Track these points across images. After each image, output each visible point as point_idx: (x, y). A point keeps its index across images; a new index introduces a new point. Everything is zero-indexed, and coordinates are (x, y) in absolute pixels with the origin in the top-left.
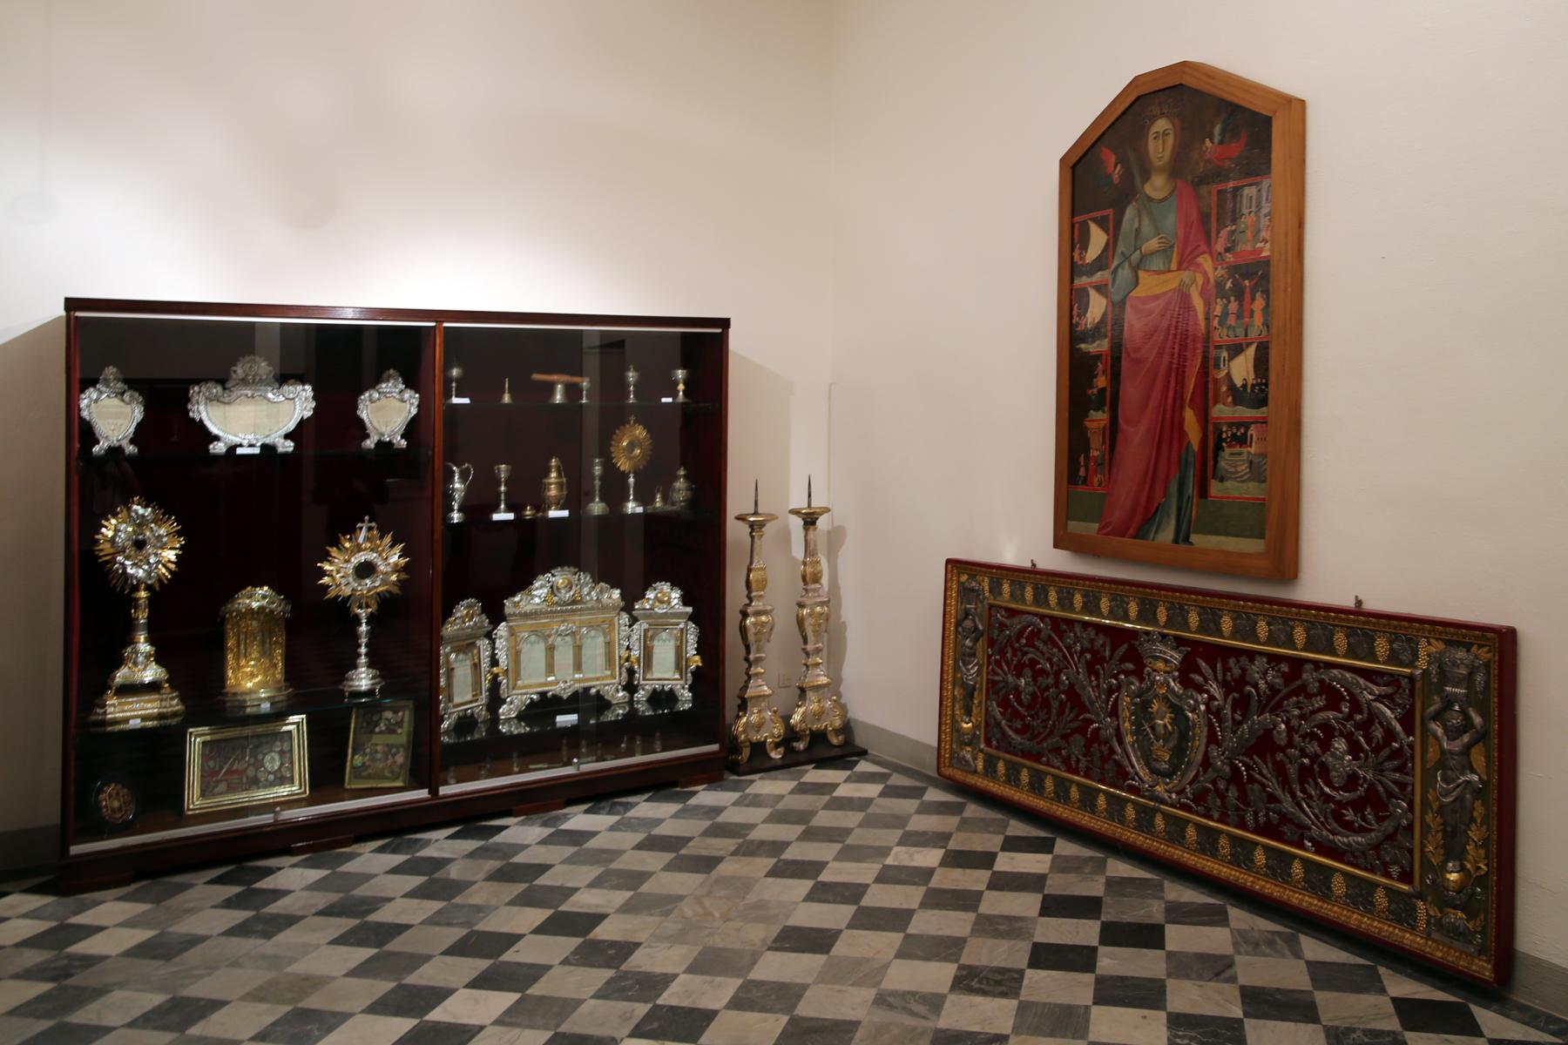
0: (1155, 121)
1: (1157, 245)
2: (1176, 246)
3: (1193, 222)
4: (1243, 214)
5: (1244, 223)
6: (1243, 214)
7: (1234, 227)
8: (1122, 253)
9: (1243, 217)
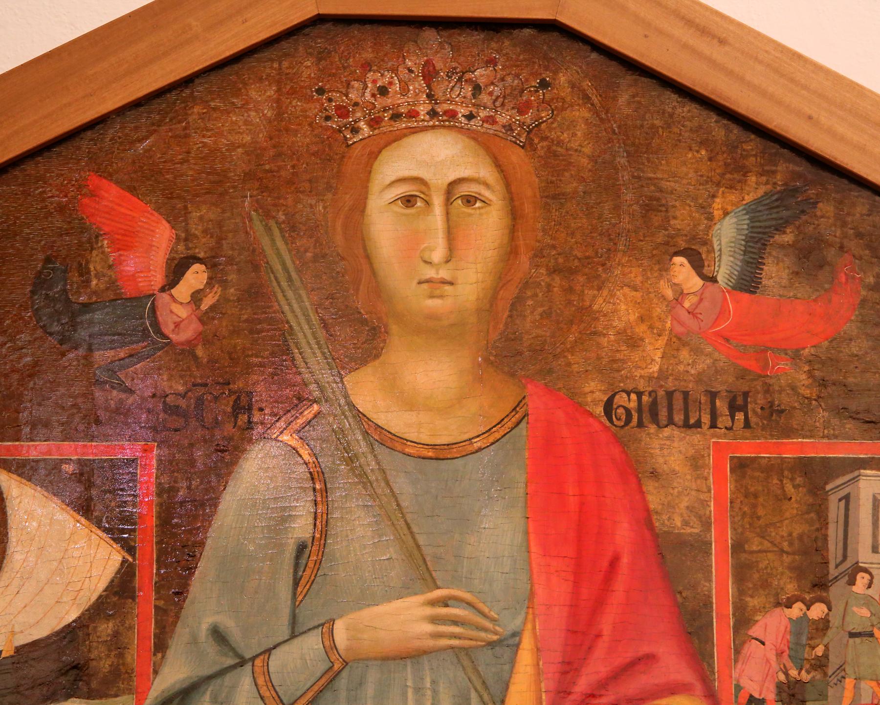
0: (399, 137)
1: (429, 628)
2: (527, 643)
3: (614, 562)
4: (857, 569)
5: (868, 601)
6: (857, 569)
7: (817, 611)
8: (218, 635)
9: (862, 579)
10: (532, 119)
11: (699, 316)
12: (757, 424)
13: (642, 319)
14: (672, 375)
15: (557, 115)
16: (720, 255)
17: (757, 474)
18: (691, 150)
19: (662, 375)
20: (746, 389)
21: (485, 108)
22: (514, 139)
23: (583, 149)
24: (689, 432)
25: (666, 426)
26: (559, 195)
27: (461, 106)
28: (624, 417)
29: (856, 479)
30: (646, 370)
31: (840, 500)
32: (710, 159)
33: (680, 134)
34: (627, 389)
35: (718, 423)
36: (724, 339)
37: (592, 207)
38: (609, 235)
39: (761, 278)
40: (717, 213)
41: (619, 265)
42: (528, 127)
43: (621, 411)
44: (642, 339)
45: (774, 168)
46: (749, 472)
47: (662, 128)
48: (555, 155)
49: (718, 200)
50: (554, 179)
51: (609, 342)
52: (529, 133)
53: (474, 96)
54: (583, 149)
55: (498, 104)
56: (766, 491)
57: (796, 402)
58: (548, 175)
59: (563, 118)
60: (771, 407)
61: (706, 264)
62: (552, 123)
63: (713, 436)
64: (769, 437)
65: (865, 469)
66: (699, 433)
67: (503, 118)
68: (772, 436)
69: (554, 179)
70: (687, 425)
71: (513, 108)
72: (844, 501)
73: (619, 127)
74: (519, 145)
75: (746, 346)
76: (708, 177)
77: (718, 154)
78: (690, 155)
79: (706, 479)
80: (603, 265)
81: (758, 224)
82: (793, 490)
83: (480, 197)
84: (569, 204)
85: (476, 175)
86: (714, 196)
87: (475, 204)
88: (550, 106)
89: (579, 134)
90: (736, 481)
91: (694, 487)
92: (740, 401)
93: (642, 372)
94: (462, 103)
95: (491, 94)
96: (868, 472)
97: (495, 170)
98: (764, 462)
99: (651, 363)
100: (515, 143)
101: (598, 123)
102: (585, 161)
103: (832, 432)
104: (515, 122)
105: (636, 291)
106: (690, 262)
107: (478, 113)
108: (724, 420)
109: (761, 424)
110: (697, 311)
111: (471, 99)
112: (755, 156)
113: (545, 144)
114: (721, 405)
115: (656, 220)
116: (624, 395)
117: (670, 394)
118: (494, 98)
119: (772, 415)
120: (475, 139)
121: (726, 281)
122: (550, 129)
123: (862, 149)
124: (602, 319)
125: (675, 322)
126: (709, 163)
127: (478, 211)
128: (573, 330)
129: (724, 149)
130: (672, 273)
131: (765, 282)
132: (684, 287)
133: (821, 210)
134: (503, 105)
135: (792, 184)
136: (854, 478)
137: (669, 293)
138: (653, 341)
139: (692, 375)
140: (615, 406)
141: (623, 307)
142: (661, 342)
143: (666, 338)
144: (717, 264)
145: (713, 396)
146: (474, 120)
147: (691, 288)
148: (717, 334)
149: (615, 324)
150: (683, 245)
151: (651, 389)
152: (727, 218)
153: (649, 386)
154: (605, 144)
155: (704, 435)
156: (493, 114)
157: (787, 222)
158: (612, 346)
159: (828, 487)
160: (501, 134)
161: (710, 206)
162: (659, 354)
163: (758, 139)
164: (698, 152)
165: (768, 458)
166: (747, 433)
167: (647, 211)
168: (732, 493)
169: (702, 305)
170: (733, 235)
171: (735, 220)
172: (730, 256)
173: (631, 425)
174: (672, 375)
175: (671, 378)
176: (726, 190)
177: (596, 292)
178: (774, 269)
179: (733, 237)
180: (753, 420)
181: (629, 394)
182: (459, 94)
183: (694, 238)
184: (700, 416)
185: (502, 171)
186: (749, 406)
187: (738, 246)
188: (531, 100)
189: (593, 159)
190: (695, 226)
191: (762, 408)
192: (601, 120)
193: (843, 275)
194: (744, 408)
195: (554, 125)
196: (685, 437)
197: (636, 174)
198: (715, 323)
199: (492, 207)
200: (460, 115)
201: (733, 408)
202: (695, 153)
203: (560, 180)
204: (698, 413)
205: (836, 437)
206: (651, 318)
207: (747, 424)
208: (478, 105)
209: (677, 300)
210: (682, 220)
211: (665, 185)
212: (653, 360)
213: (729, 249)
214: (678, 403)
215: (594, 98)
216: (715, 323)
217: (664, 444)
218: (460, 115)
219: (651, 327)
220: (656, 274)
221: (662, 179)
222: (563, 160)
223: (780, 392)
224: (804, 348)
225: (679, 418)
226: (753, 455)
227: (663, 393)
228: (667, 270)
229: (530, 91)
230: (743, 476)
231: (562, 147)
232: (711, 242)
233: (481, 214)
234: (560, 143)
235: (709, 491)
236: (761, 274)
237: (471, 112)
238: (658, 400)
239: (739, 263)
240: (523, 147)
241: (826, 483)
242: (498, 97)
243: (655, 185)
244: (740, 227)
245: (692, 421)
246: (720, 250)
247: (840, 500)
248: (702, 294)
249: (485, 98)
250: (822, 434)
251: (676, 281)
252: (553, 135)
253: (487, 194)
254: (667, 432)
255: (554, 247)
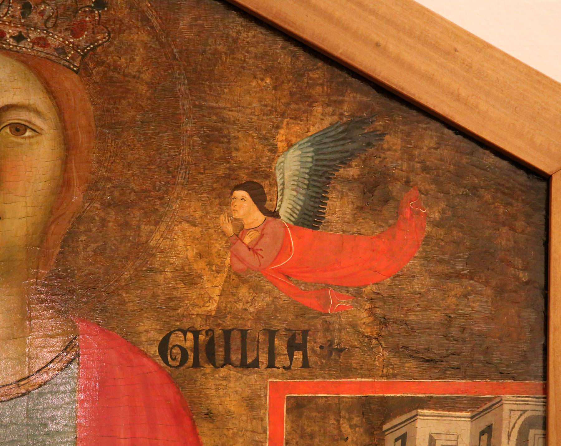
10: (86, 42)
11: (259, 252)
12: (316, 363)
13: (200, 255)
14: (230, 313)
15: (114, 38)
16: (283, 189)
17: (314, 414)
18: (255, 78)
19: (220, 313)
20: (306, 328)
21: (36, 29)
22: (67, 64)
23: (142, 76)
24: (246, 372)
25: (223, 366)
26: (115, 124)
27: (10, 25)
28: (179, 357)
29: (413, 419)
30: (204, 309)
31: (396, 440)
32: (275, 88)
33: (245, 61)
34: (183, 328)
35: (276, 362)
36: (285, 276)
37: (151, 138)
38: (168, 167)
39: (324, 213)
40: (281, 145)
41: (177, 199)
42: (83, 51)
43: (176, 350)
44: (200, 277)
45: (341, 98)
46: (306, 412)
47: (226, 54)
48: (112, 81)
49: (282, 131)
50: (110, 107)
51: (165, 279)
52: (83, 57)
53: (23, 15)
54: (142, 76)
55: (49, 24)
56: (322, 431)
57: (356, 340)
58: (104, 102)
59: (121, 42)
60: (330, 345)
61: (268, 198)
62: (109, 47)
63: (271, 376)
64: (327, 376)
65: (423, 408)
66: (256, 373)
67: (55, 40)
68: (331, 376)
69: (110, 107)
70: (244, 365)
71: (66, 29)
72: (400, 441)
73: (180, 52)
74: (73, 70)
75: (306, 283)
76: (272, 107)
77: (283, 82)
78: (254, 84)
79: (262, 420)
80: (161, 198)
81: (322, 157)
82: (349, 430)
83: (31, 126)
84: (125, 134)
85: (26, 102)
86: (278, 127)
87: (24, 133)
88: (107, 28)
89: (138, 59)
90: (292, 422)
91: (249, 427)
92: (299, 340)
93: (199, 311)
94: (10, 22)
95: (42, 13)
96: (426, 412)
97: (46, 96)
98: (321, 401)
99: (209, 301)
100: (69, 67)
101: (158, 47)
102: (143, 89)
103: (391, 371)
104: (68, 45)
105: (195, 225)
106: (251, 196)
107: (28, 34)
108: (282, 360)
109: (319, 363)
110: (258, 247)
111: (20, 19)
112: (322, 85)
113: (101, 69)
114: (280, 344)
115: (217, 151)
116: (181, 334)
117: (227, 334)
118: (45, 17)
119: (331, 354)
120: (23, 62)
121: (289, 216)
122: (107, 54)
123: (430, 79)
124: (159, 255)
125: (235, 259)
126: (274, 92)
127: (28, 141)
128: (128, 267)
129: (290, 77)
130: (233, 208)
131: (328, 217)
132: (245, 222)
133: (388, 143)
134: (55, 25)
135: (359, 114)
136: (411, 418)
137: (229, 229)
138: (211, 278)
139: (251, 313)
140: (170, 346)
141: (181, 243)
142: (221, 279)
143: (225, 275)
144: (279, 199)
145: (272, 334)
146: (23, 42)
147: (253, 223)
148: (279, 271)
149: (172, 261)
150: (244, 177)
151: (208, 328)
152: (291, 151)
153: (206, 325)
154: (165, 71)
155: (262, 374)
156: (45, 36)
157: (352, 155)
158: (169, 283)
159: (385, 427)
160: (53, 58)
161: (274, 137)
162: (217, 291)
163: (326, 67)
164: (262, 80)
165: (326, 397)
166: (306, 372)
167: (208, 142)
168: (288, 434)
169: (263, 240)
170: (296, 168)
171: (299, 152)
172: (293, 190)
173: (187, 365)
174: (230, 313)
175: (229, 316)
176: (291, 121)
177: (153, 227)
178: (338, 204)
179: (297, 170)
180: (312, 358)
181: (185, 333)
182: (7, 13)
183: (256, 171)
184: (258, 355)
185: (55, 98)
186: (308, 345)
187: (301, 179)
188: (86, 21)
189: (151, 85)
190: (257, 158)
191: (321, 347)
192: (161, 44)
193: (407, 210)
194: (302, 347)
195: (111, 49)
196: (242, 377)
197: (197, 103)
198: (276, 260)
199: (43, 136)
200: (8, 36)
201: (292, 347)
202: (259, 81)
203: (117, 109)
204: (256, 352)
205: (395, 376)
206: (210, 254)
207: (306, 364)
208: (27, 26)
209: (237, 236)
210: (245, 152)
211: (228, 114)
212: (211, 298)
213: (292, 183)
214: (236, 343)
215: (153, 20)
216: (276, 260)
217: (221, 385)
218: (8, 36)
219: (210, 264)
220: (216, 209)
221: (225, 108)
222: (121, 87)
223: (340, 331)
224: (366, 286)
225: (236, 357)
226: (310, 395)
227: (221, 332)
228: (228, 204)
229: (85, 11)
230: (300, 416)
231: (119, 73)
232: (274, 175)
233: (31, 144)
234: (116, 68)
235: (265, 432)
236: (325, 209)
237: (20, 32)
238: (215, 339)
239: (302, 198)
240: (76, 72)
241: (383, 423)
242: (49, 17)
243: (216, 114)
244: (304, 160)
245: (249, 361)
246: (283, 184)
247: (396, 440)
248: (263, 229)
249: (35, 18)
250: (381, 373)
251: (236, 215)
252: (110, 59)
253: (38, 122)
254: (223, 371)
255: (109, 179)
